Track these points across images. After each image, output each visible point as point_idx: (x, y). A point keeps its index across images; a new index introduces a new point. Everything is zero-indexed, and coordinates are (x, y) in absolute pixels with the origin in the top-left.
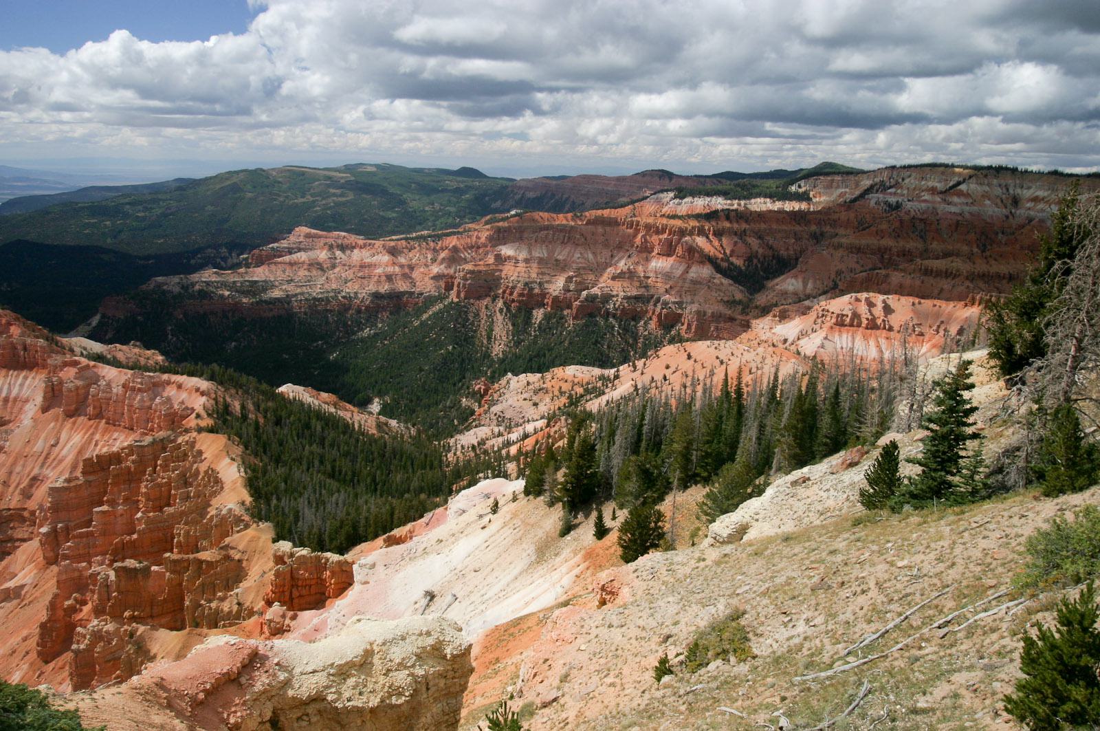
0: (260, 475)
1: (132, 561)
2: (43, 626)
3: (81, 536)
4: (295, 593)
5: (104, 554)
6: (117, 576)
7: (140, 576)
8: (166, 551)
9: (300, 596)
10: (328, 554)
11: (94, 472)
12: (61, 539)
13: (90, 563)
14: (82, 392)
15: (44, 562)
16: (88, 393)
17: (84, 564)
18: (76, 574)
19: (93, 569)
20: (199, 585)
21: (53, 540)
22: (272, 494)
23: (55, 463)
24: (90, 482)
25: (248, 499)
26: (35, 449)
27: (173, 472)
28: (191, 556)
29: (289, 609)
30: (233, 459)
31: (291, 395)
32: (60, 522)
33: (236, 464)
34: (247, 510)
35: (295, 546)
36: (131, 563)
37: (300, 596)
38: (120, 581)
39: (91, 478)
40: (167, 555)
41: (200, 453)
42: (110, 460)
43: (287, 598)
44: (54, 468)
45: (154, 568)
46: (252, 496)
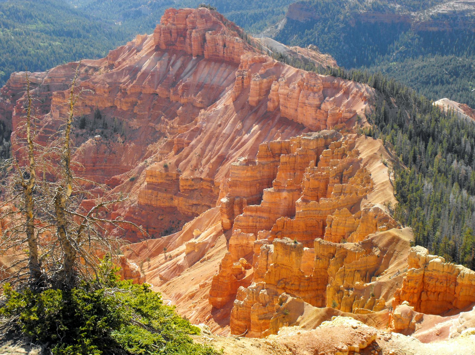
0: (407, 181)
1: (289, 239)
2: (216, 279)
3: (251, 210)
4: (424, 297)
5: (268, 229)
6: (276, 250)
7: (294, 253)
8: (318, 236)
9: (428, 300)
10: (461, 267)
11: (267, 157)
12: (236, 209)
13: (256, 234)
14: (264, 86)
15: (220, 228)
16: (269, 88)
17: (251, 235)
18: (245, 242)
19: (258, 240)
20: (341, 272)
21: (231, 211)
22: (416, 201)
23: (239, 144)
24: (263, 165)
25: (394, 202)
26: (224, 131)
27: (332, 166)
28: (338, 245)
29: (416, 310)
30: (385, 164)
31: (446, 109)
32: (238, 197)
33: (386, 169)
34: (392, 212)
35: (430, 252)
36: (288, 241)
37: (428, 300)
38: (278, 255)
39: (264, 161)
40: (318, 239)
41: (358, 153)
42: (281, 149)
43: (416, 299)
44: (237, 150)
45: (305, 249)
46: (398, 200)
